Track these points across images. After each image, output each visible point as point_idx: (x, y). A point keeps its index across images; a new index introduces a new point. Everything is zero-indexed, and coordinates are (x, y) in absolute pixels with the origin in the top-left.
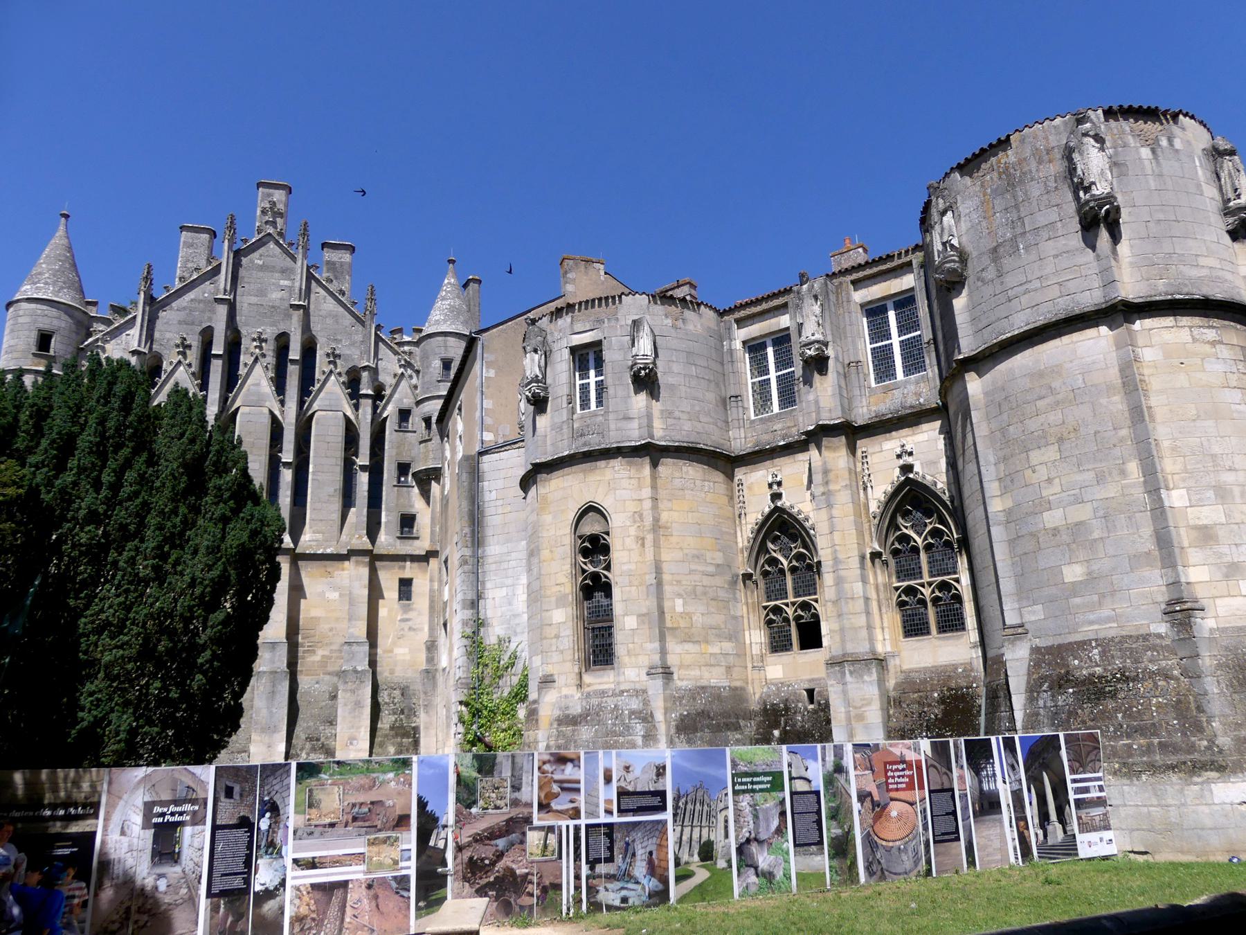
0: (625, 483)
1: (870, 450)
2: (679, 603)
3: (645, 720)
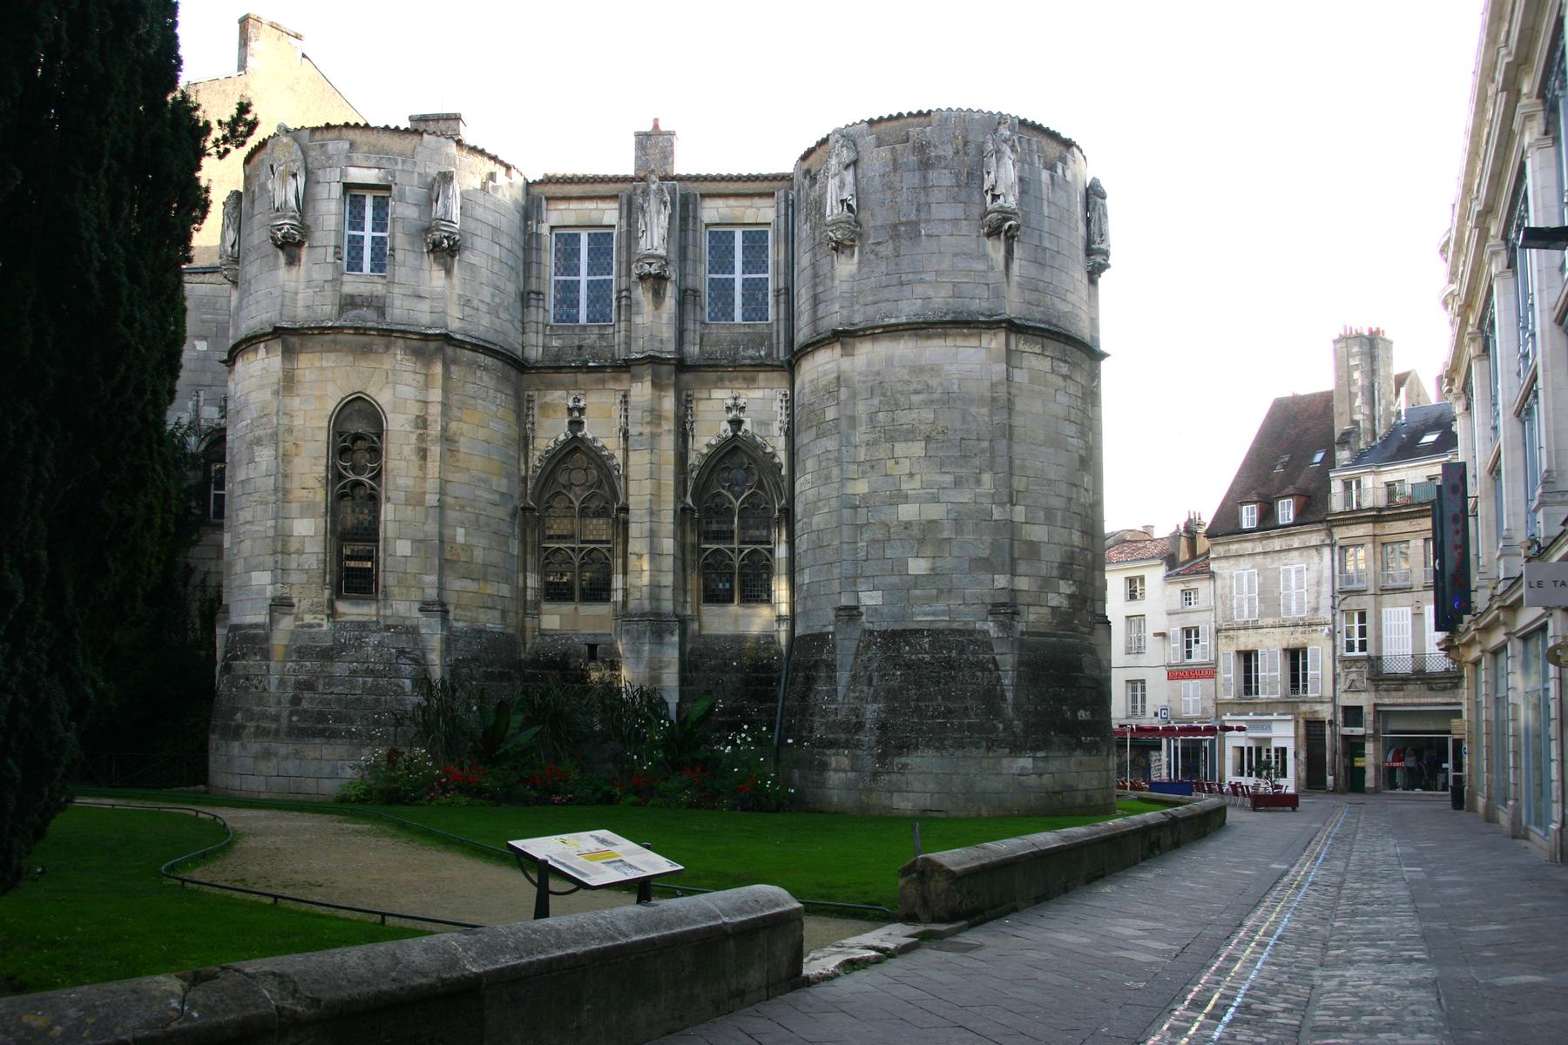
0: (408, 377)
1: (697, 395)
2: (460, 532)
3: (416, 661)
